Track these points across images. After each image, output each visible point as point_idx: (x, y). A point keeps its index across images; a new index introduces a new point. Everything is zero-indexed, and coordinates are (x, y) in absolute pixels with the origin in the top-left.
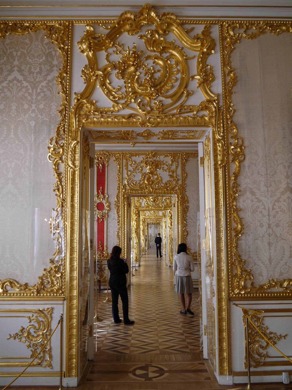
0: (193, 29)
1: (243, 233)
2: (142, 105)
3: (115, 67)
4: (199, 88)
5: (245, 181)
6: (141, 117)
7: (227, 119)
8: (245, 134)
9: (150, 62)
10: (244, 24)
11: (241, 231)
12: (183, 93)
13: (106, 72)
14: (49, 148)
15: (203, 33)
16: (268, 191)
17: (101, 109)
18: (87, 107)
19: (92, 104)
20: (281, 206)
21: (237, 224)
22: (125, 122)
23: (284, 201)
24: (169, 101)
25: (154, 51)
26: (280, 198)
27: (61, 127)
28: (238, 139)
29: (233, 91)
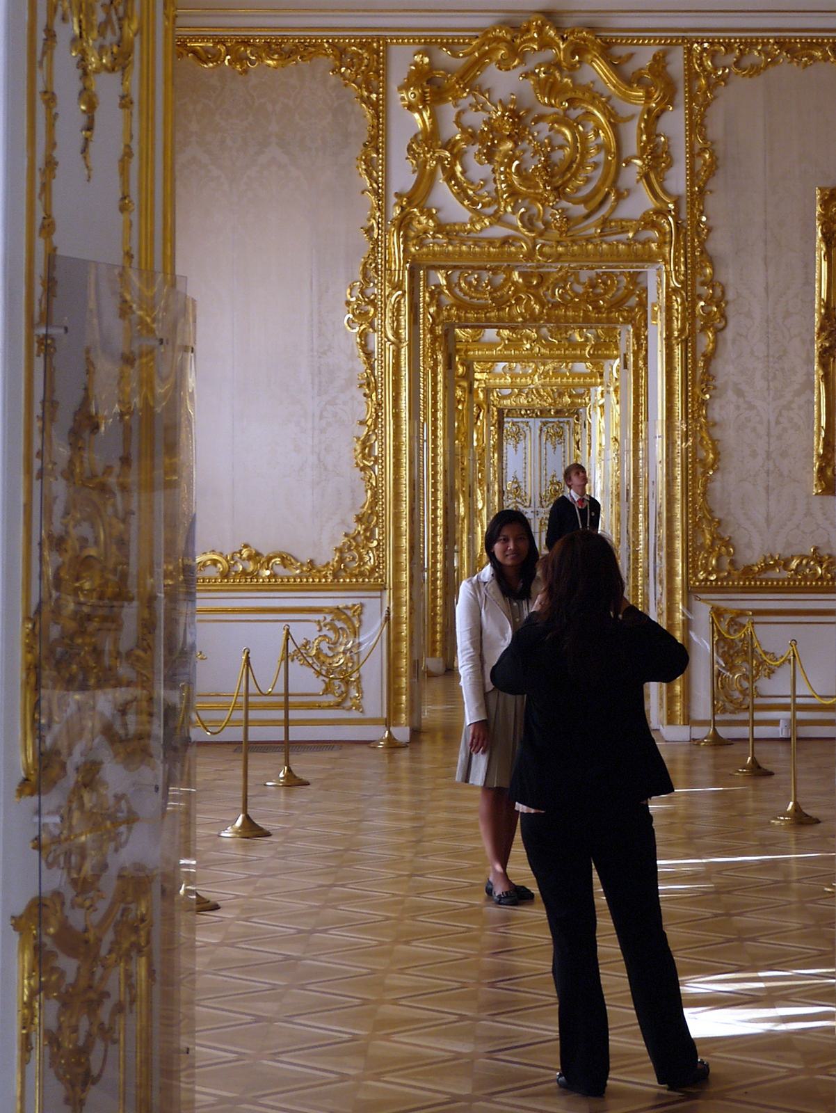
0: (631, 55)
1: (718, 469)
2: (529, 222)
3: (472, 137)
4: (641, 183)
5: (725, 370)
6: (526, 243)
7: (694, 249)
8: (728, 275)
9: (544, 126)
10: (736, 45)
11: (713, 465)
12: (608, 194)
13: (455, 150)
14: (348, 303)
15: (651, 68)
16: (768, 389)
17: (448, 228)
18: (420, 223)
19: (430, 216)
20: (792, 419)
21: (707, 451)
22: (495, 254)
23: (800, 407)
24: (581, 210)
25: (552, 106)
26: (791, 402)
27: (370, 261)
28: (713, 287)
29: (708, 188)
